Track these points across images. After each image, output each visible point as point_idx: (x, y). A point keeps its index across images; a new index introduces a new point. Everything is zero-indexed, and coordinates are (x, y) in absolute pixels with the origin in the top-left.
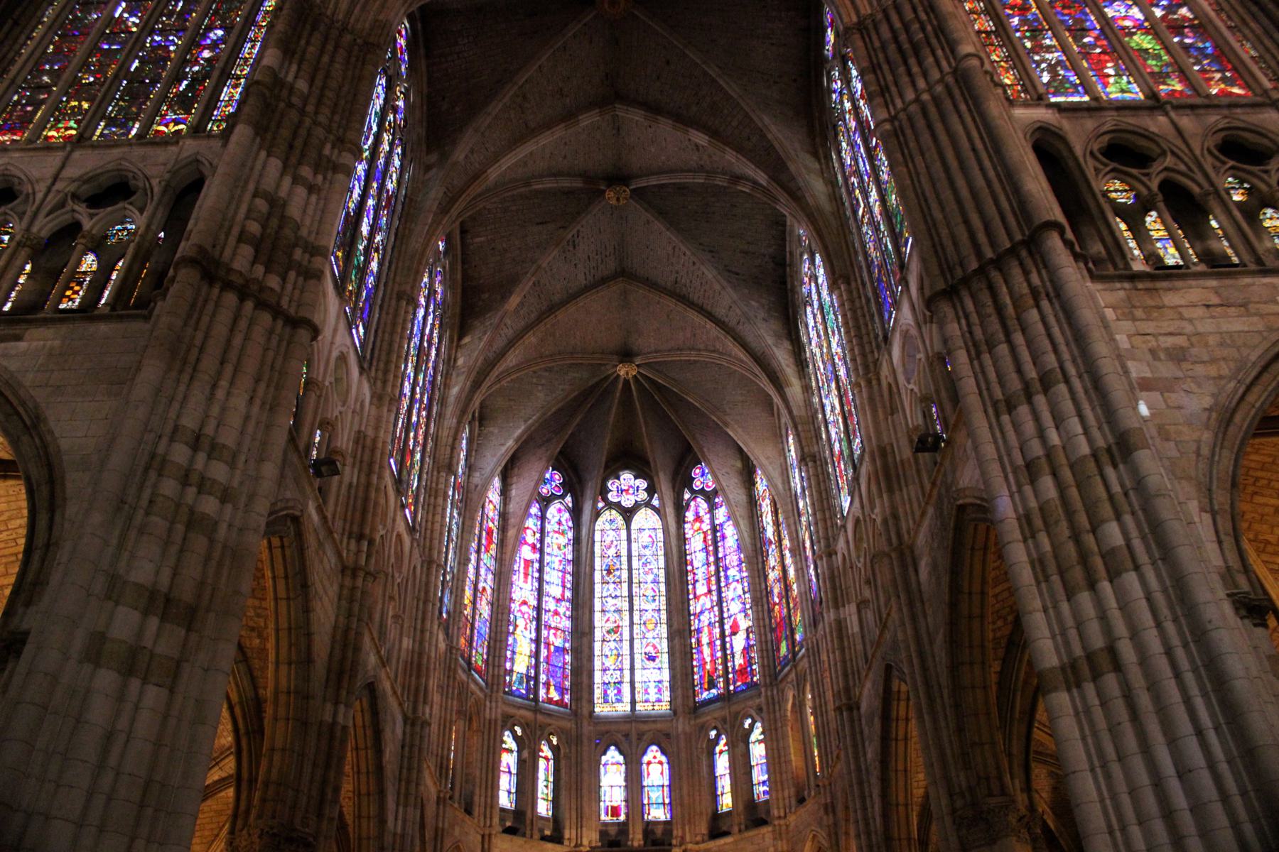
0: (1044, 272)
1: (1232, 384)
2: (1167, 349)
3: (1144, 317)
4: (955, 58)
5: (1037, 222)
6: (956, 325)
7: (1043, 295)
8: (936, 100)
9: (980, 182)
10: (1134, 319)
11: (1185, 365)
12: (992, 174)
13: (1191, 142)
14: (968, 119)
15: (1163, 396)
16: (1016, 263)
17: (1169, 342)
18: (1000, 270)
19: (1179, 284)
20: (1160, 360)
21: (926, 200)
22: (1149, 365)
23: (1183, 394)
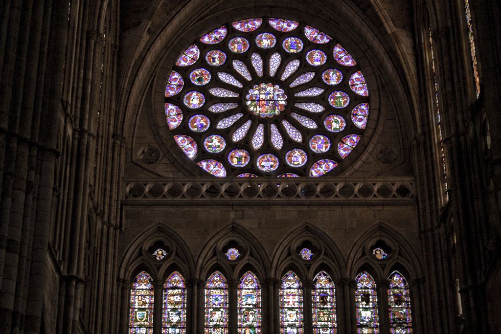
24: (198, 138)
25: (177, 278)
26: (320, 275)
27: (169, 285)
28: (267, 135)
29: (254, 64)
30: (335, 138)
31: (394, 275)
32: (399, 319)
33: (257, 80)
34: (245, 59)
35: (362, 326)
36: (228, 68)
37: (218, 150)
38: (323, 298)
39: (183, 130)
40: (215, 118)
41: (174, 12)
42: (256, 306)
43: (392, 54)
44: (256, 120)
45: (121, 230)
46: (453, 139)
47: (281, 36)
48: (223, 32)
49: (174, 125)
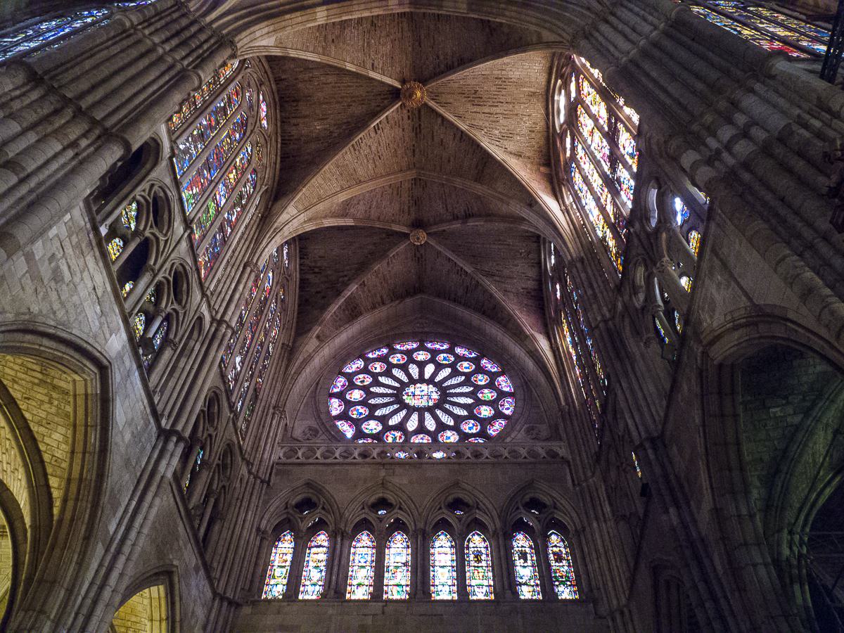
0: (92, 149)
1: (52, 323)
2: (58, 267)
3: (74, 244)
4: (194, 68)
5: (126, 136)
6: (11, 87)
7: (76, 151)
8: (160, 59)
9: (128, 93)
10: (69, 236)
11: (53, 284)
12: (137, 101)
13: (176, 251)
14: (161, 82)
15: (26, 272)
16: (87, 128)
17: (64, 268)
18: (74, 117)
19: (101, 264)
20: (50, 263)
21: (92, 56)
22: (45, 255)
23: (33, 288)
24: (357, 423)
25: (322, 539)
26: (474, 535)
27: (313, 544)
28: (421, 420)
29: (411, 371)
30: (485, 422)
31: (551, 534)
32: (562, 577)
33: (412, 381)
34: (404, 368)
35: (521, 584)
36: (388, 373)
37: (374, 432)
38: (478, 556)
39: (344, 416)
40: (373, 408)
41: (342, 328)
42: (405, 564)
43: (535, 355)
44: (411, 410)
45: (268, 485)
46: (601, 325)
47: (434, 353)
48: (385, 351)
49: (334, 413)
